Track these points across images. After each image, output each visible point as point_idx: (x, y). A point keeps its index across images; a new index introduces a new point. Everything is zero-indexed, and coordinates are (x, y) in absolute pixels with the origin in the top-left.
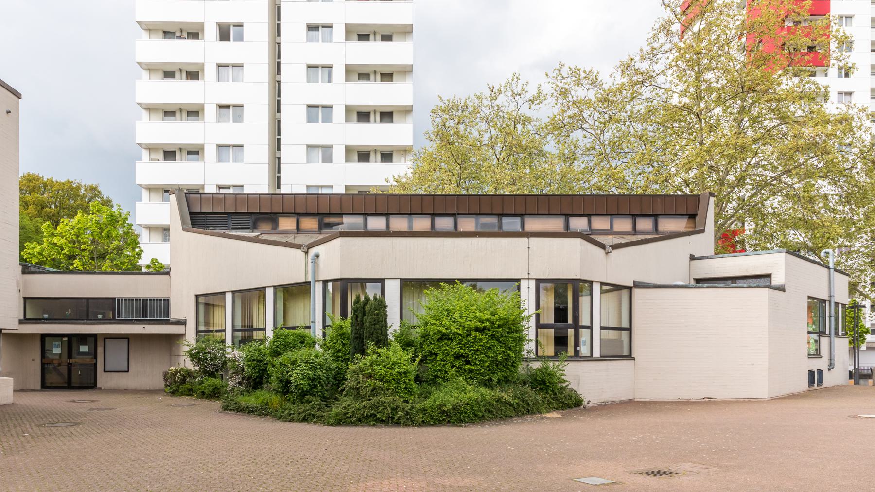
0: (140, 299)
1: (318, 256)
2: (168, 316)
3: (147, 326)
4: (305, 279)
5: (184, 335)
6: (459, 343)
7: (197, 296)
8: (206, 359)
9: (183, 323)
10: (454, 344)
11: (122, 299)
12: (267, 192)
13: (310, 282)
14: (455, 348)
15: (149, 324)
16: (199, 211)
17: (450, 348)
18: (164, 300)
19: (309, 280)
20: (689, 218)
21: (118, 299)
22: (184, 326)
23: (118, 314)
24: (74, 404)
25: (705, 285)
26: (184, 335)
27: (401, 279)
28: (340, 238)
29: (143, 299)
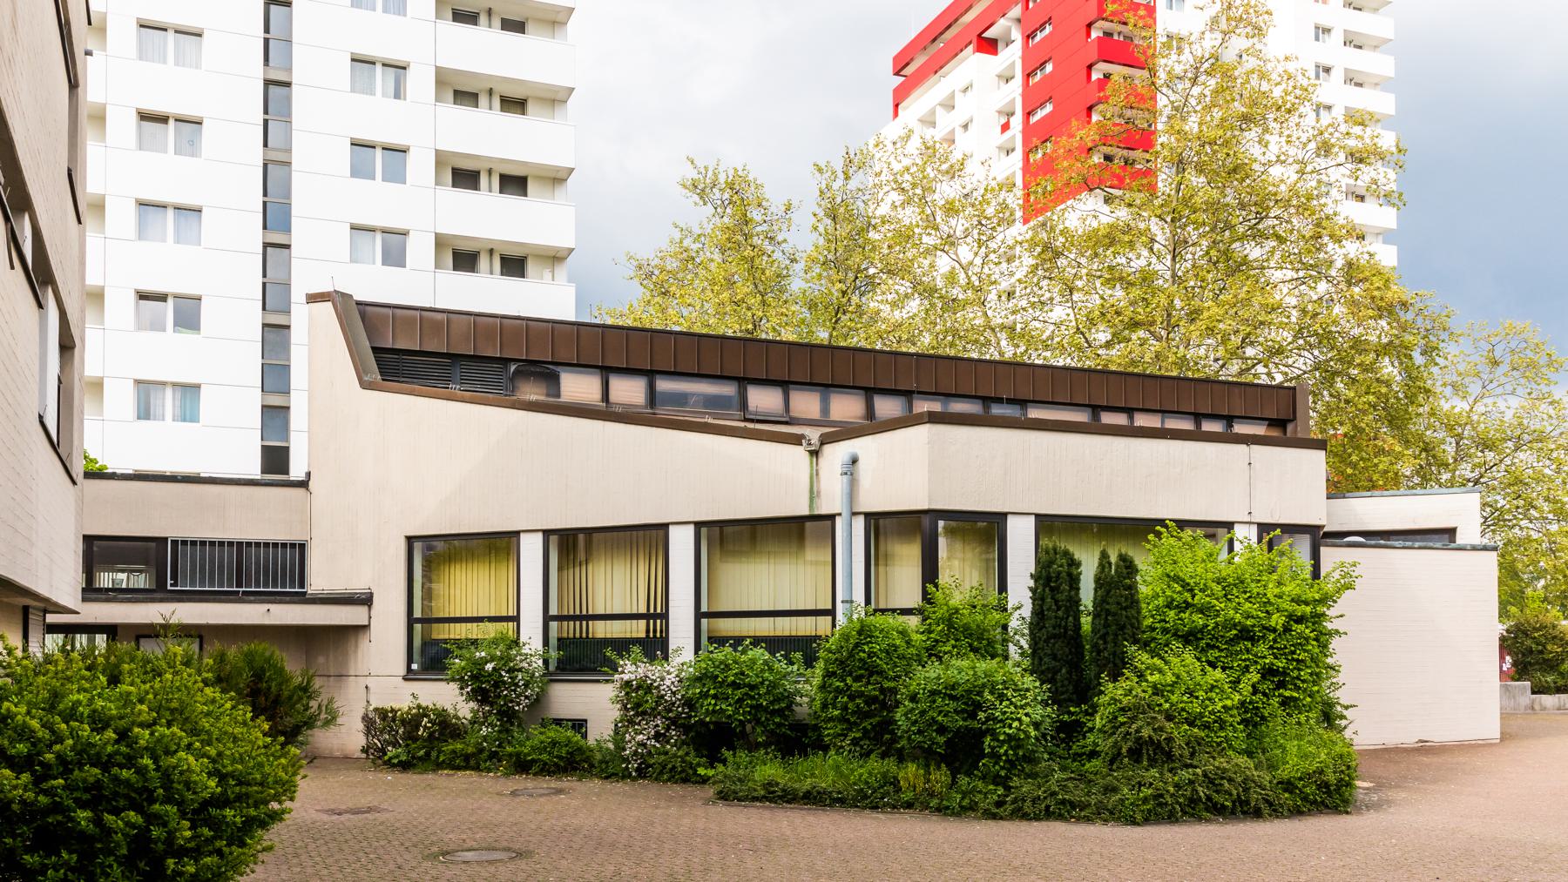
0: (231, 544)
1: (854, 461)
2: (302, 585)
3: (274, 607)
4: (811, 506)
5: (365, 628)
6: (1271, 648)
7: (410, 540)
8: (517, 685)
9: (366, 600)
10: (1262, 648)
11: (184, 543)
12: (573, 319)
13: (831, 518)
14: (1265, 657)
15: (280, 602)
16: (390, 346)
17: (1256, 656)
18: (293, 545)
19: (824, 509)
20: (1269, 425)
21: (175, 542)
22: (366, 608)
23: (174, 577)
24: (364, 802)
25: (1396, 544)
26: (365, 628)
27: (1037, 516)
28: (928, 425)
29: (240, 544)
